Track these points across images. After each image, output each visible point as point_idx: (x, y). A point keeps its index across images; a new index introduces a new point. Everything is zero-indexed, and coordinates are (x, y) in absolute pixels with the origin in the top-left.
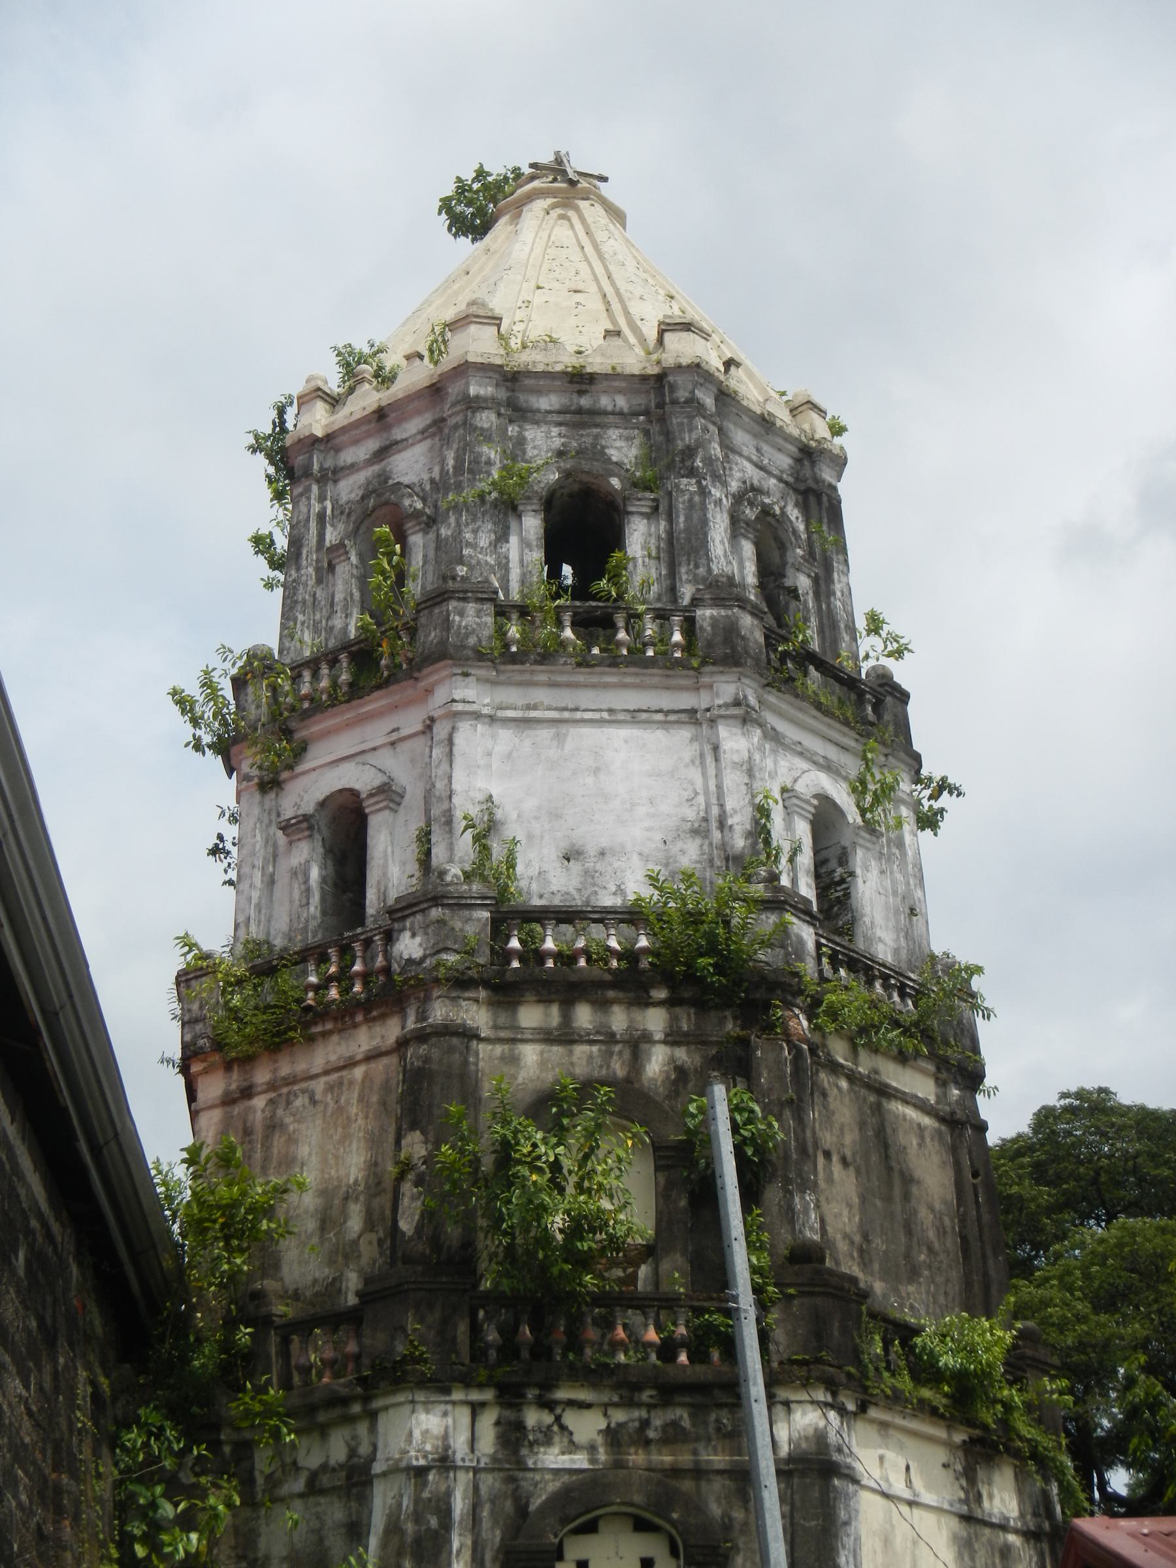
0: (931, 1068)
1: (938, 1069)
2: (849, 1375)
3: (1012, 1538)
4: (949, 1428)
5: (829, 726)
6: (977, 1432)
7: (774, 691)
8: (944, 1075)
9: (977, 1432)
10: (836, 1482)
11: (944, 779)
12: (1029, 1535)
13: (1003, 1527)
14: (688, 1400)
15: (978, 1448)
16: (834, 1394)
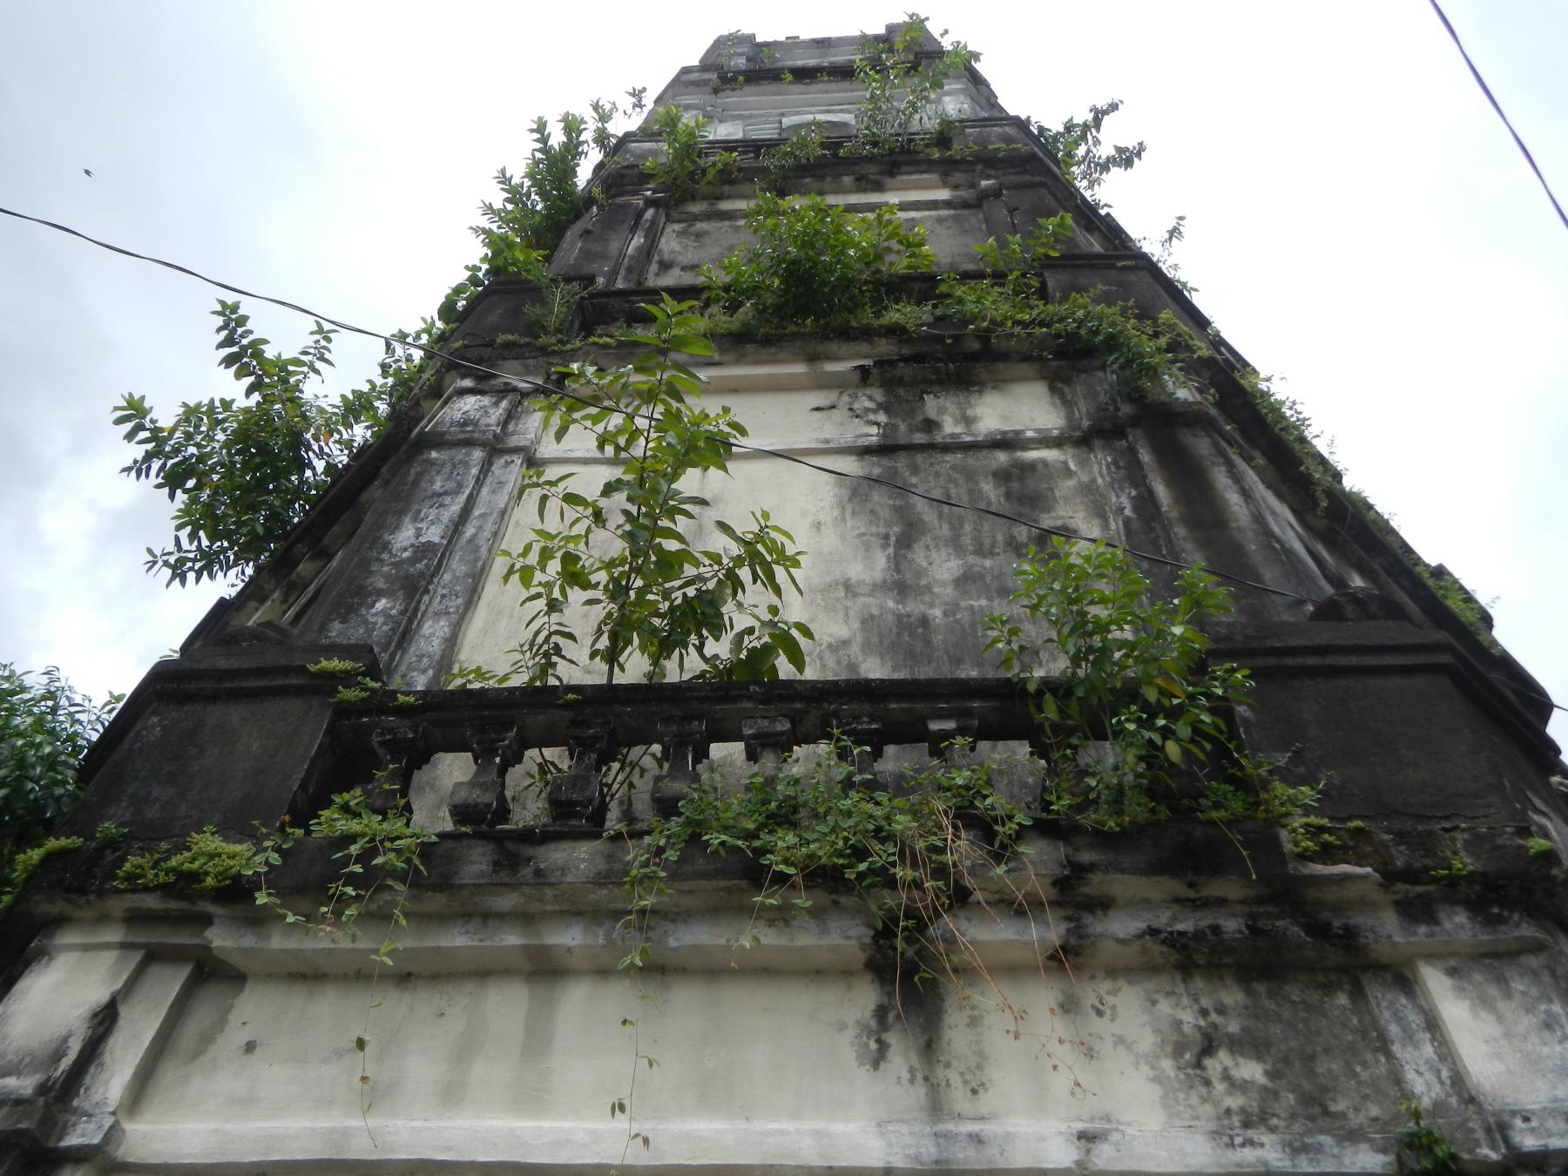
0: (932, 177)
1: (945, 175)
2: (507, 346)
3: (1033, 455)
4: (812, 359)
5: (827, 92)
6: (885, 347)
7: (728, 93)
8: (958, 177)
9: (885, 347)
10: (434, 454)
11: (1094, 109)
12: (1082, 439)
13: (1007, 442)
14: (336, 528)
15: (903, 370)
16: (482, 378)
